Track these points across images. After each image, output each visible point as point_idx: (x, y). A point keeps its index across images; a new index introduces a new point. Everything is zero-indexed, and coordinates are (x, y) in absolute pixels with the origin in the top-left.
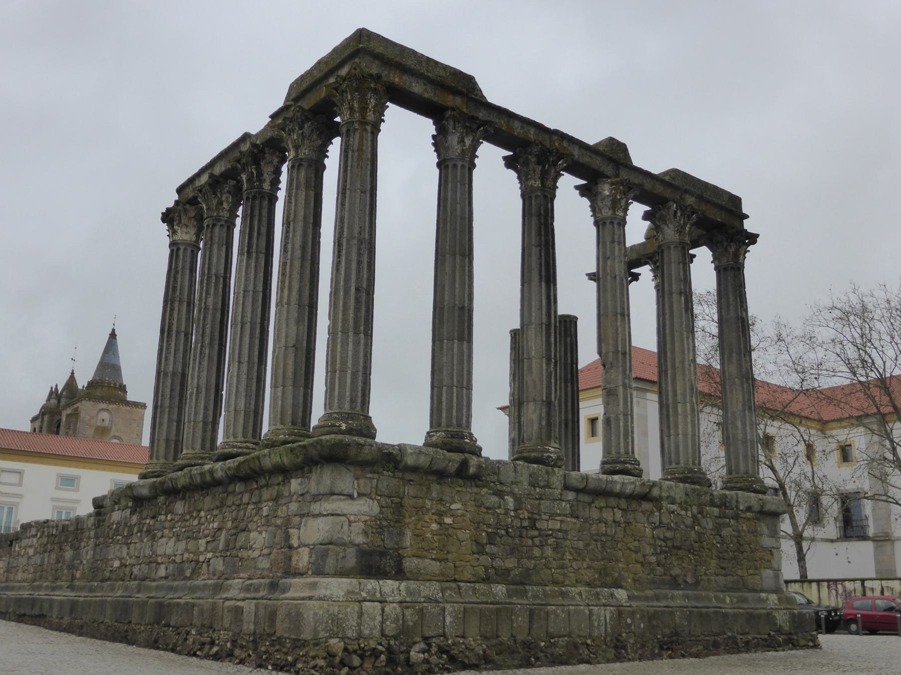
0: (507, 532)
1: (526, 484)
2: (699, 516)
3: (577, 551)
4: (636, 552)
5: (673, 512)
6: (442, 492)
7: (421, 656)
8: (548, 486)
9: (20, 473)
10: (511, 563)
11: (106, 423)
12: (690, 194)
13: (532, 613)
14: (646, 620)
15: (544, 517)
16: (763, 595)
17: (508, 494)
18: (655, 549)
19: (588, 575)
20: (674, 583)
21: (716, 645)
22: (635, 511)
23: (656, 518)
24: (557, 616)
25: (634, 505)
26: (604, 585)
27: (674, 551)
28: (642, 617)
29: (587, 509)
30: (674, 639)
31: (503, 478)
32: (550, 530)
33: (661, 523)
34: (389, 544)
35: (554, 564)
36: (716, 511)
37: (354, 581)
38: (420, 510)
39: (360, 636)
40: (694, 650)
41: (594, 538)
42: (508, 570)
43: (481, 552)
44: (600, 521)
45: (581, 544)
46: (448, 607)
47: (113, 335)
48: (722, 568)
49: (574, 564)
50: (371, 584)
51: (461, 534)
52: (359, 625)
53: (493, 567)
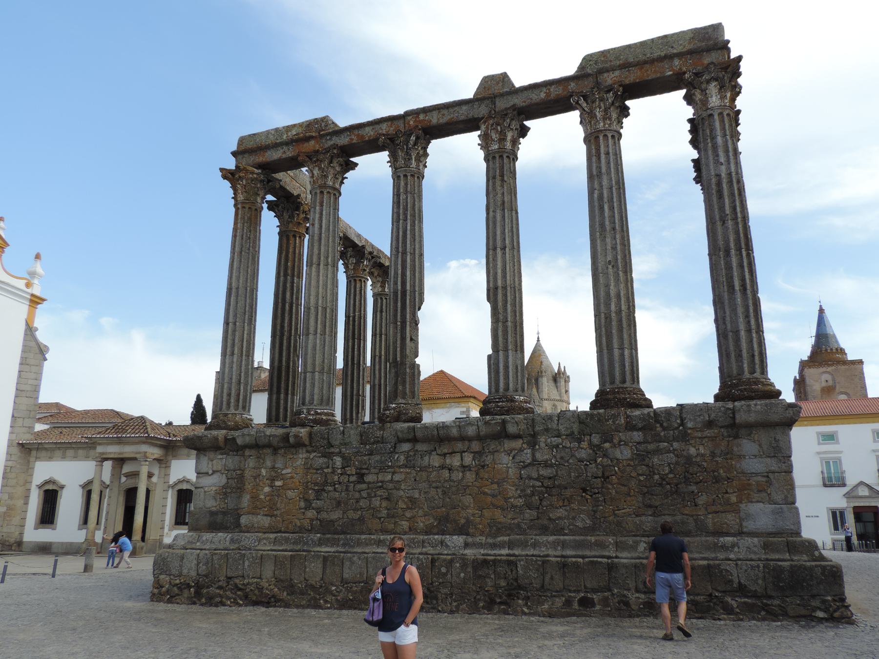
0: (335, 490)
1: (355, 444)
2: (607, 445)
4: (493, 496)
5: (557, 446)
6: (275, 461)
7: (218, 591)
10: (335, 515)
11: (830, 383)
12: (608, 71)
13: (325, 559)
14: (470, 569)
15: (373, 470)
21: (585, 603)
24: (352, 563)
26: (443, 533)
28: (464, 566)
29: (427, 457)
30: (514, 592)
31: (333, 442)
32: (382, 482)
33: (534, 459)
34: (231, 506)
36: (637, 436)
37: (194, 534)
41: (434, 485)
42: (332, 521)
43: (307, 508)
44: (442, 467)
47: (821, 311)
48: (650, 506)
49: (408, 514)
51: (290, 494)
52: (181, 566)
53: (317, 519)
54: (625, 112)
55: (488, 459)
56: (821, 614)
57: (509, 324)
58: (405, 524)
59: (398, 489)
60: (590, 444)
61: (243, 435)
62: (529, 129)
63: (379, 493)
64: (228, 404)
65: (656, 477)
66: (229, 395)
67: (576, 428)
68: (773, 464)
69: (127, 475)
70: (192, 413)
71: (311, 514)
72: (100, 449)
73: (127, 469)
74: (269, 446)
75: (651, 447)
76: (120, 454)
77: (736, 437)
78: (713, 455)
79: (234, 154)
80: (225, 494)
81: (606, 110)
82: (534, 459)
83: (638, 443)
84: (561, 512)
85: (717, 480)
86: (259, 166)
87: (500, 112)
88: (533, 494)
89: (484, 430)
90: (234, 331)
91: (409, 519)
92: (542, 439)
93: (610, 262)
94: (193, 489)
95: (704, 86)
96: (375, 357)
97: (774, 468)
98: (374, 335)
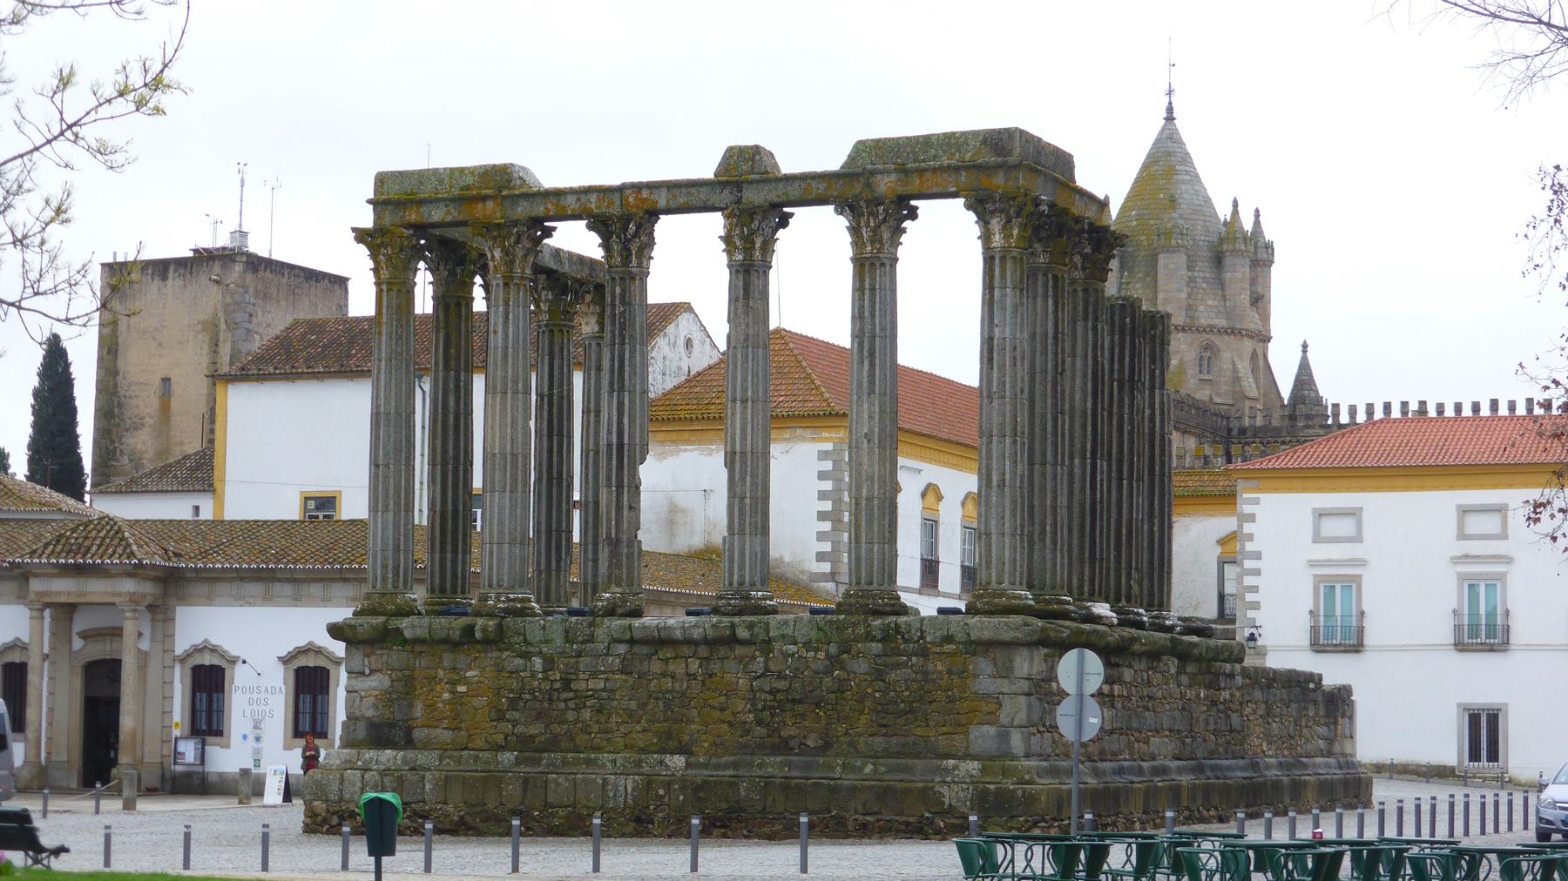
1: (559, 642)
3: (630, 713)
4: (722, 710)
8: (591, 639)
10: (533, 730)
13: (526, 781)
16: (951, 762)
18: (754, 705)
19: (641, 740)
20: (783, 747)
22: (722, 659)
24: (558, 785)
25: (723, 651)
26: (663, 751)
27: (788, 706)
28: (683, 789)
33: (767, 670)
34: (399, 716)
35: (596, 728)
36: (876, 647)
37: (354, 751)
38: (433, 679)
39: (341, 800)
40: (766, 830)
44: (664, 674)
45: (633, 704)
46: (428, 775)
49: (622, 728)
50: (370, 754)
51: (477, 702)
52: (341, 790)
54: (913, 214)
57: (747, 501)
58: (621, 742)
60: (827, 655)
61: (413, 626)
64: (384, 579)
66: (384, 567)
69: (85, 636)
70: (37, 394)
72: (36, 585)
73: (81, 623)
74: (447, 641)
76: (78, 596)
77: (974, 654)
78: (950, 672)
79: (369, 202)
81: (876, 230)
82: (767, 670)
84: (793, 731)
86: (410, 226)
87: (751, 199)
88: (764, 709)
89: (711, 633)
90: (386, 477)
92: (777, 646)
94: (223, 664)
96: (588, 451)
98: (585, 453)
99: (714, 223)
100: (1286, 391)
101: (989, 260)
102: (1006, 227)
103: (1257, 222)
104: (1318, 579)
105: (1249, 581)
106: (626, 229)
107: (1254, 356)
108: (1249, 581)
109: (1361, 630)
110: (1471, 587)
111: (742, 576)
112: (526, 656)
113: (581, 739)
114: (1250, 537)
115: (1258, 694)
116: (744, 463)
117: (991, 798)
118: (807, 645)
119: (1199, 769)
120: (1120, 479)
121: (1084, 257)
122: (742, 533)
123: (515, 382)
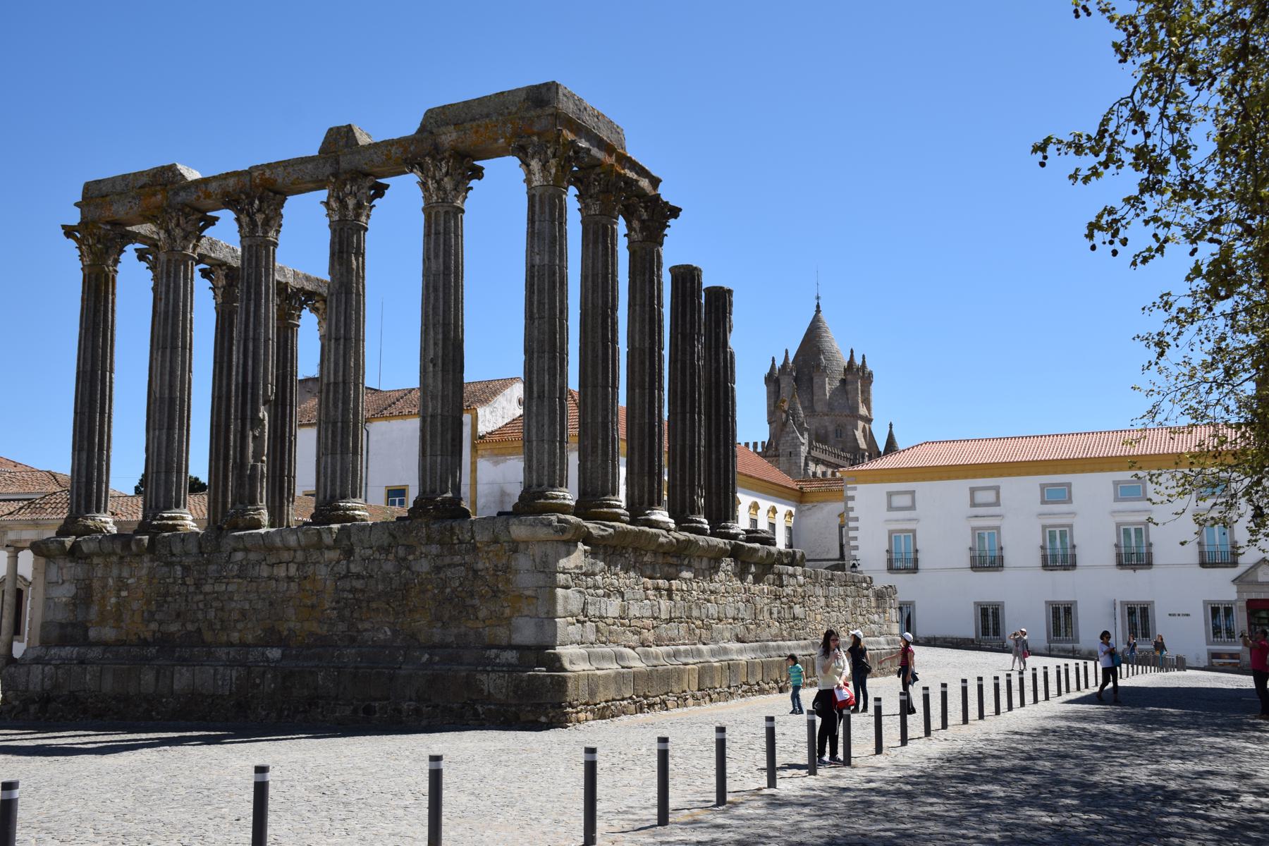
2: (411, 557)
9: (997, 489)
10: (174, 628)
16: (493, 652)
17: (180, 563)
18: (338, 602)
22: (314, 564)
23: (342, 568)
25: (315, 556)
31: (175, 551)
34: (80, 618)
36: (435, 549)
39: (27, 690)
44: (270, 578)
49: (240, 626)
52: (27, 681)
55: (310, 570)
56: (543, 719)
59: (231, 599)
62: (387, 186)
63: (215, 604)
64: (78, 506)
65: (448, 590)
67: (386, 539)
68: (540, 579)
71: (154, 626)
75: (447, 560)
77: (515, 551)
78: (496, 569)
79: (76, 205)
80: (74, 604)
82: (348, 571)
83: (437, 556)
84: (367, 625)
85: (496, 593)
87: (349, 172)
91: (240, 631)
92: (357, 550)
93: (432, 360)
95: (528, 160)
97: (541, 583)
99: (323, 194)
100: (882, 448)
101: (531, 199)
102: (544, 168)
103: (864, 362)
104: (891, 533)
105: (852, 534)
106: (252, 204)
107: (864, 430)
108: (852, 534)
109: (916, 560)
110: (978, 534)
111: (333, 490)
112: (170, 564)
113: (208, 636)
114: (852, 509)
115: (819, 591)
116: (336, 392)
117: (524, 684)
118: (381, 549)
119: (765, 649)
120: (684, 413)
121: (642, 222)
122: (334, 453)
123: (174, 338)
